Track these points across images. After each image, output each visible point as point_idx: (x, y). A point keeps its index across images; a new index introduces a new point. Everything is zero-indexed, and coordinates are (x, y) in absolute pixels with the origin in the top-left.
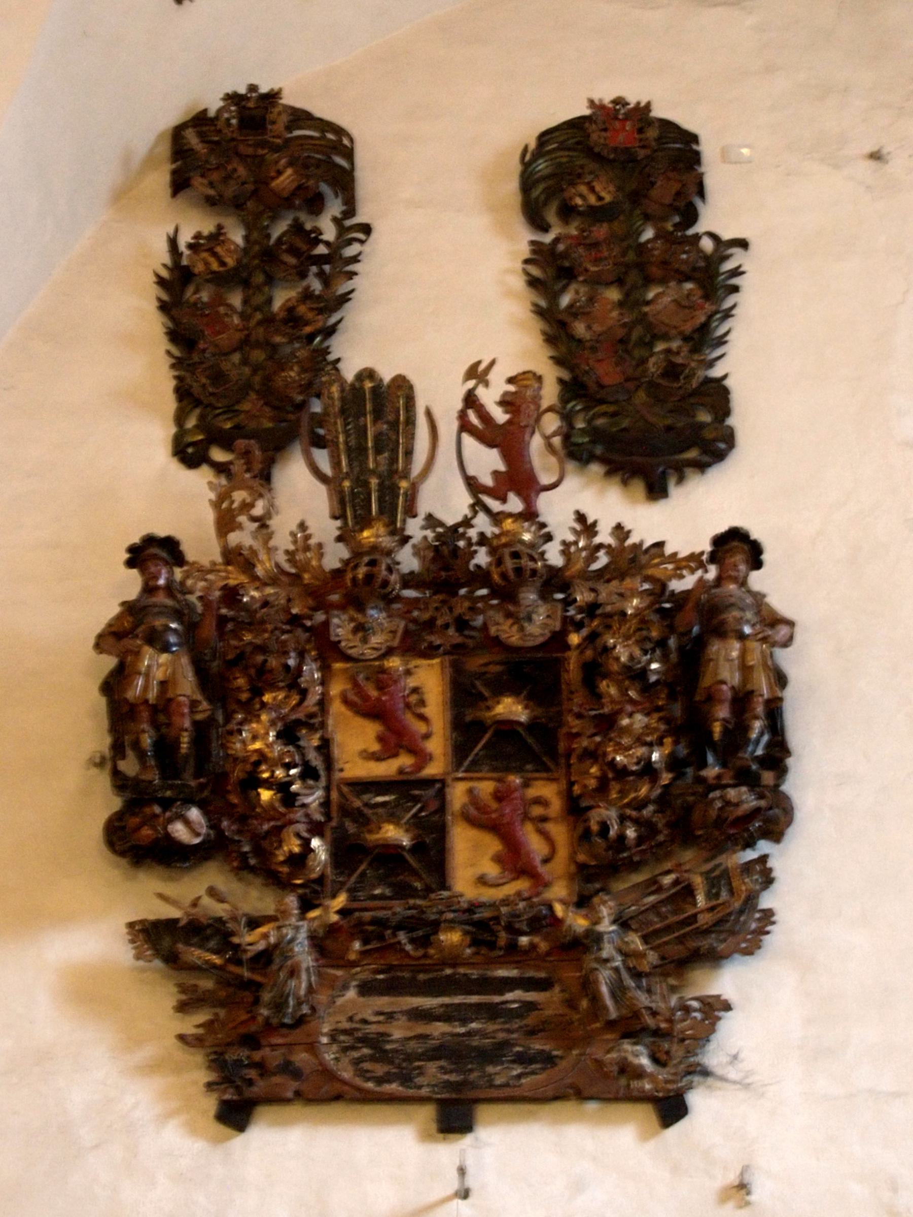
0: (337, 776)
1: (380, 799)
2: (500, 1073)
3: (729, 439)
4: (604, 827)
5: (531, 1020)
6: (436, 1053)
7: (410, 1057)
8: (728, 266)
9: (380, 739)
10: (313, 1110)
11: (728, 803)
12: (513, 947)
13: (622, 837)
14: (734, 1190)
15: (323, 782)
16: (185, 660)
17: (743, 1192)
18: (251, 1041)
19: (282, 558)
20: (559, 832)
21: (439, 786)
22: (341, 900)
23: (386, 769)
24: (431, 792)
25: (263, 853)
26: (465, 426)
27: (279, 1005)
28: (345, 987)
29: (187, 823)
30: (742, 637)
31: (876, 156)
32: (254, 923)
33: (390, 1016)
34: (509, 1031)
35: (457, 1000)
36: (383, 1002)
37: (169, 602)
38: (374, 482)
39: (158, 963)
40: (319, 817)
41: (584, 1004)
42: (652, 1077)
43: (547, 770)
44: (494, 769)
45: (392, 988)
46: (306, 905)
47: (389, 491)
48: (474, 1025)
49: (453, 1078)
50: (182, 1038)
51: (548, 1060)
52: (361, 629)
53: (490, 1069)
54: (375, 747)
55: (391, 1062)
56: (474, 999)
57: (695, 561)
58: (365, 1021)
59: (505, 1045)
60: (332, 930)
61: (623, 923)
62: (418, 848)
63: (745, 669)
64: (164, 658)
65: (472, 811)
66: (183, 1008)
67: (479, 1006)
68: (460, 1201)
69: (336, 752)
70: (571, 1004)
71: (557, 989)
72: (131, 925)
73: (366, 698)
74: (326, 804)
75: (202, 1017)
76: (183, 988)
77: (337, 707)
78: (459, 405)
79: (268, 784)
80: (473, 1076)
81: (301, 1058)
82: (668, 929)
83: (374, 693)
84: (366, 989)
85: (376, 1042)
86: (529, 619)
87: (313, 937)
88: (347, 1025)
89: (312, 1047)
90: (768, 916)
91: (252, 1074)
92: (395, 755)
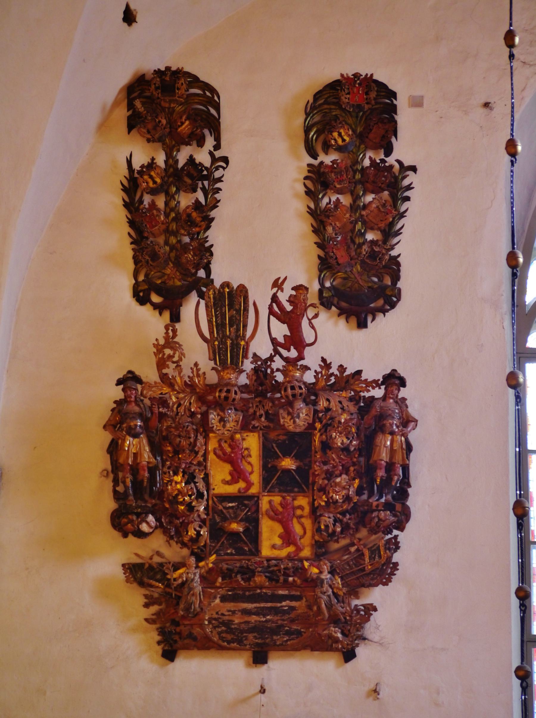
0: (212, 492)
1: (230, 505)
2: (279, 639)
3: (398, 295)
4: (327, 526)
5: (292, 615)
6: (252, 630)
7: (242, 632)
8: (406, 182)
9: (231, 474)
10: (202, 652)
11: (380, 519)
12: (286, 581)
13: (334, 532)
14: (373, 692)
15: (206, 497)
16: (145, 441)
17: (376, 694)
18: (177, 624)
19: (187, 380)
20: (308, 523)
21: (256, 499)
22: (213, 558)
23: (232, 489)
24: (253, 502)
25: (178, 533)
26: (271, 312)
27: (187, 609)
28: (215, 598)
29: (148, 523)
30: (392, 433)
31: (486, 105)
32: (176, 567)
33: (234, 612)
34: (284, 620)
35: (262, 605)
36: (231, 606)
37: (137, 409)
38: (229, 342)
39: (135, 585)
40: (204, 516)
41: (315, 608)
42: (341, 642)
43: (304, 491)
44: (280, 491)
45: (235, 598)
46: (199, 559)
47: (235, 346)
48: (268, 617)
49: (259, 641)
50: (146, 620)
51: (299, 633)
52: (222, 420)
53: (275, 637)
54: (229, 478)
55: (234, 634)
56: (269, 605)
57: (376, 384)
58: (223, 615)
59: (282, 626)
60: (210, 570)
61: (332, 572)
62: (246, 530)
63: (392, 452)
64: (136, 441)
65: (272, 513)
66: (146, 606)
67: (271, 608)
68: (262, 695)
69: (211, 480)
70: (310, 607)
71: (304, 599)
72: (123, 565)
73: (225, 453)
74: (206, 509)
75: (154, 609)
76: (146, 596)
77: (211, 456)
78: (269, 301)
79: (182, 503)
80: (267, 641)
81: (197, 631)
82: (353, 573)
83: (228, 450)
84: (224, 599)
85: (227, 624)
86: (298, 417)
87: (202, 577)
88: (216, 616)
89: (201, 626)
90: (396, 564)
91: (176, 637)
92: (237, 482)
